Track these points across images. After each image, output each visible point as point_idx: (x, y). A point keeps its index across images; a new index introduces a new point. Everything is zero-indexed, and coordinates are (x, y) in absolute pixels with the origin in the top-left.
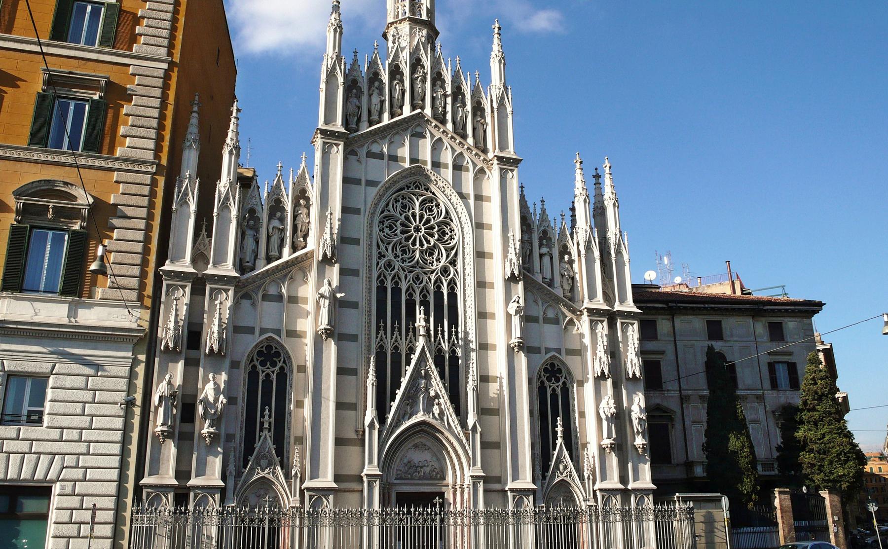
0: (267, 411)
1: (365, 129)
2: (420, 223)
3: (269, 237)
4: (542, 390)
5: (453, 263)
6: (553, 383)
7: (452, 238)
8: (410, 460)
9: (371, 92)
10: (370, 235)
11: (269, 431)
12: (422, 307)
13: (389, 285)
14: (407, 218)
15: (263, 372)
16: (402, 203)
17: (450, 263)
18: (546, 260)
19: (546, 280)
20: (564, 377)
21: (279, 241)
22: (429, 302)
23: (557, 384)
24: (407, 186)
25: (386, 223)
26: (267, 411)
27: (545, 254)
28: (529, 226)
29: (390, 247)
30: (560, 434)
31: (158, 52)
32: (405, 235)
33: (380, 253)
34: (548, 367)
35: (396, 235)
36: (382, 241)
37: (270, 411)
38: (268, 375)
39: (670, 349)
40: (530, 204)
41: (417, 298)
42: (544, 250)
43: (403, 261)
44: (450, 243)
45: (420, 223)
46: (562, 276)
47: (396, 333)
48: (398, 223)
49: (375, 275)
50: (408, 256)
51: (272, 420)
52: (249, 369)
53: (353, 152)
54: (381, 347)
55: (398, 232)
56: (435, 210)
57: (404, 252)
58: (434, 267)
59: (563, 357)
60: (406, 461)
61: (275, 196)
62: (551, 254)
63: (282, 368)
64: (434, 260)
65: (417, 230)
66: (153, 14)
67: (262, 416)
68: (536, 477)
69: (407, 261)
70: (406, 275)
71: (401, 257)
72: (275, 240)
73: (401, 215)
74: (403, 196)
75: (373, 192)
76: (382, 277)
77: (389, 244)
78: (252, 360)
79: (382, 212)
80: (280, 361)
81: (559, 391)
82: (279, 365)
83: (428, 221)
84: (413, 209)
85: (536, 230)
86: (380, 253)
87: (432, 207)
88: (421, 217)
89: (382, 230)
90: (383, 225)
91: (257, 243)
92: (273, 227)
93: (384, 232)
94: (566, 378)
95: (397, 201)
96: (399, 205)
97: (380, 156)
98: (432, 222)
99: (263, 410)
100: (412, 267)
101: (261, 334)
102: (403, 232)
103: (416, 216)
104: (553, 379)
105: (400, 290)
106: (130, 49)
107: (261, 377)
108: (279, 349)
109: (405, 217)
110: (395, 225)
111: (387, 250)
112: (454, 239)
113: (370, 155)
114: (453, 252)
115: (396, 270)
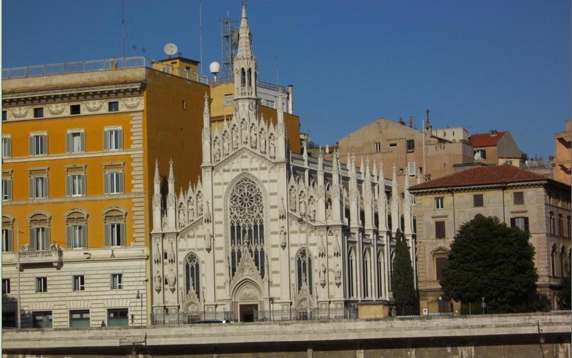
5: (262, 212)
13: (235, 225)
41: (247, 229)
43: (241, 214)
49: (229, 221)
57: (241, 210)
72: (191, 213)
75: (226, 187)
97: (229, 171)
113: (225, 171)
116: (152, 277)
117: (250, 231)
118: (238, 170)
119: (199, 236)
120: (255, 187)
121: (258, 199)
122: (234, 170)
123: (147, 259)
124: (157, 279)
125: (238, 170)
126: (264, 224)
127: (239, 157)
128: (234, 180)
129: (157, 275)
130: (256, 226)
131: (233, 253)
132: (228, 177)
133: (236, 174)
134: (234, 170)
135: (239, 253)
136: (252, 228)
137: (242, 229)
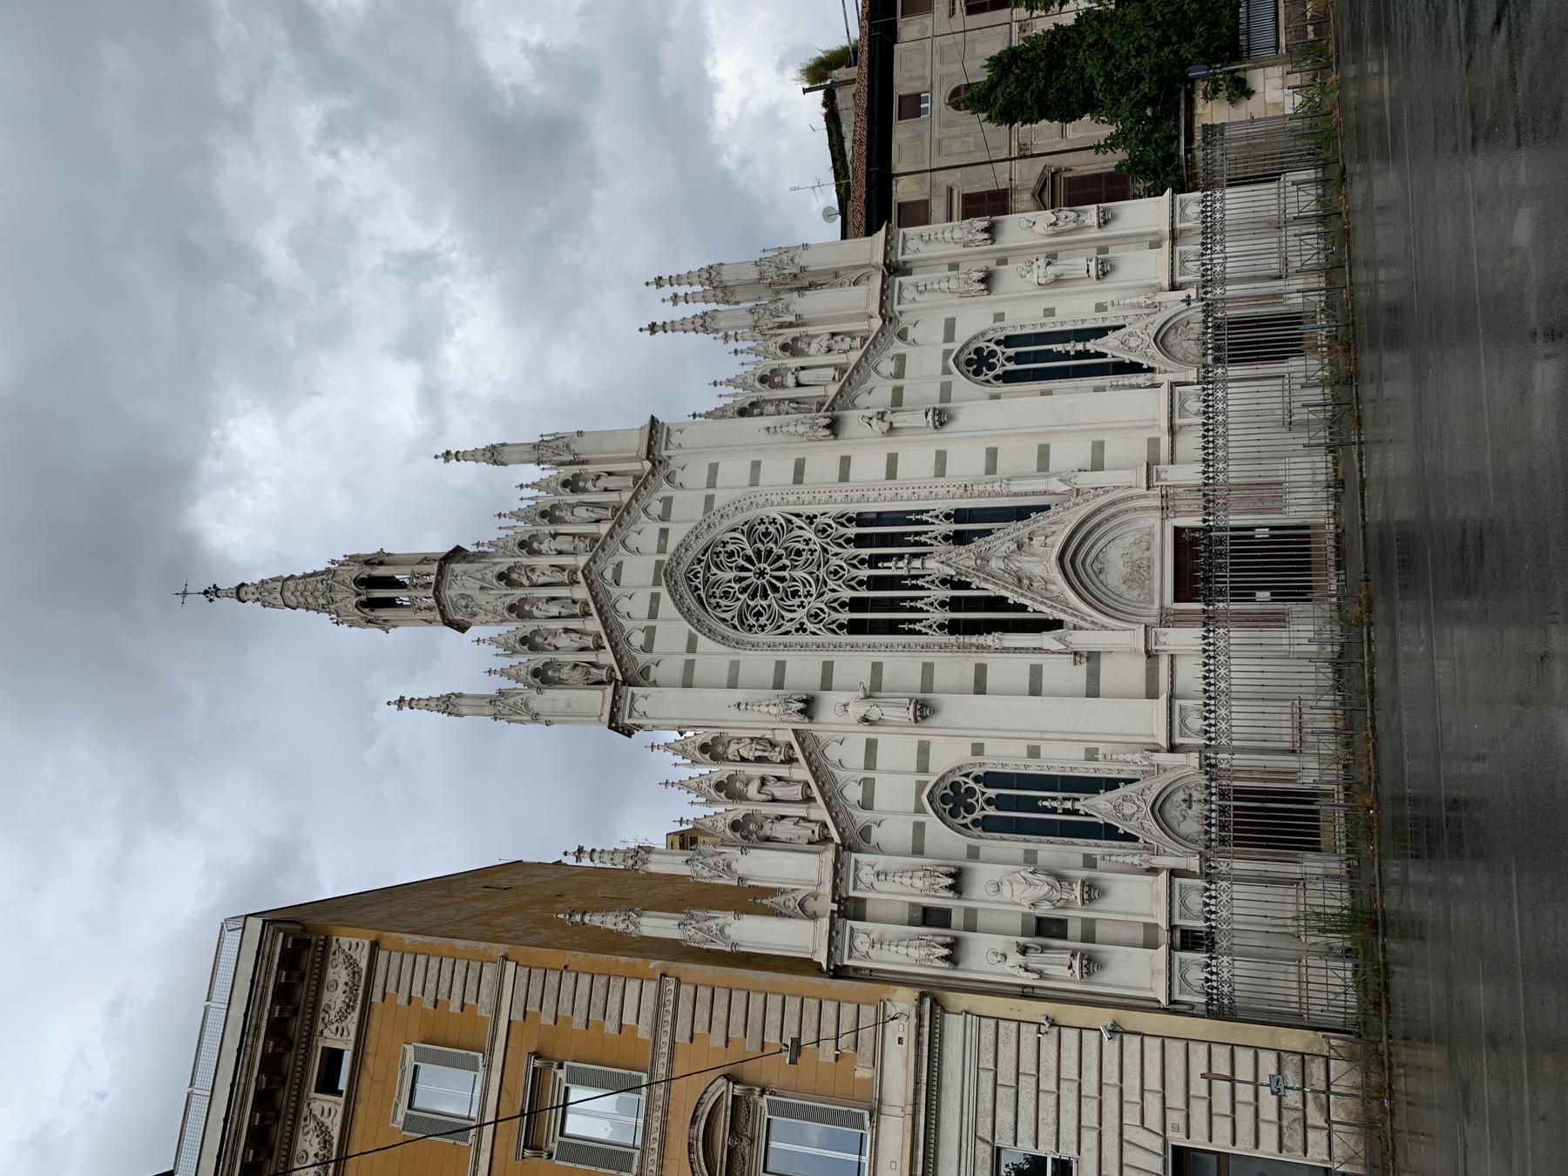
0: (1045, 803)
1: (607, 658)
2: (750, 570)
3: (774, 800)
4: (1008, 378)
5: (811, 519)
6: (998, 360)
7: (774, 522)
8: (1121, 581)
9: (550, 648)
10: (771, 646)
11: (1078, 800)
12: (880, 565)
13: (845, 616)
14: (744, 590)
15: (983, 809)
16: (721, 598)
17: (812, 523)
18: (804, 377)
19: (837, 377)
20: (988, 344)
21: (780, 783)
22: (871, 556)
23: (1000, 354)
24: (695, 591)
25: (752, 621)
26: (1045, 803)
27: (796, 378)
28: (753, 404)
29: (788, 615)
30: (1080, 347)
31: (489, 977)
32: (769, 592)
33: (797, 630)
34: (971, 369)
35: (769, 606)
36: (779, 627)
37: (1045, 799)
38: (989, 801)
39: (943, 178)
40: (720, 403)
41: (865, 573)
42: (790, 380)
43: (809, 594)
44: (781, 524)
45: (750, 570)
46: (829, 350)
47: (919, 604)
48: (752, 603)
49: (828, 638)
50: (801, 588)
51: (1060, 795)
52: (978, 831)
53: (645, 673)
54: (941, 627)
55: (764, 603)
56: (730, 547)
57: (795, 594)
58: (818, 548)
59: (956, 346)
60: (1124, 588)
61: (712, 791)
62: (796, 369)
63: (977, 779)
64: (806, 548)
65: (762, 573)
66: (431, 986)
67: (1054, 811)
68: (1149, 383)
69: (809, 588)
70: (830, 590)
71: (803, 599)
72: (778, 790)
73: (738, 599)
74: (710, 597)
75: (703, 642)
76: (833, 626)
77: (783, 617)
78: (965, 826)
79: (735, 627)
80: (966, 783)
81: (1011, 352)
82: (971, 784)
83: (748, 559)
84: (730, 581)
85: (758, 394)
86: (797, 630)
87: (726, 552)
88: (742, 569)
89: (763, 628)
90: (754, 626)
91: (783, 817)
92: (759, 792)
93: (766, 625)
94: (990, 341)
95: (718, 605)
96: (723, 602)
97: (650, 632)
98: (750, 552)
99: (1045, 810)
100: (817, 580)
101: (924, 812)
102: (765, 596)
103: (740, 577)
104: (991, 361)
105: (852, 599)
106: (485, 1019)
107: (991, 811)
109: (741, 593)
110: (754, 609)
111: (792, 620)
112: (774, 519)
114: (794, 519)
115: (823, 606)
116: (1026, 993)
117: (873, 562)
118: (655, 598)
119: (870, 763)
120: (724, 544)
121: (766, 534)
122: (653, 614)
123: (935, 1002)
124: (1034, 959)
125: (655, 598)
126: (853, 509)
127: (615, 591)
128: (687, 614)
129: (1015, 958)
130: (860, 541)
131: (953, 628)
132: (673, 629)
133: (667, 604)
134: (653, 614)
135: (954, 604)
136: (865, 552)
137: (864, 593)
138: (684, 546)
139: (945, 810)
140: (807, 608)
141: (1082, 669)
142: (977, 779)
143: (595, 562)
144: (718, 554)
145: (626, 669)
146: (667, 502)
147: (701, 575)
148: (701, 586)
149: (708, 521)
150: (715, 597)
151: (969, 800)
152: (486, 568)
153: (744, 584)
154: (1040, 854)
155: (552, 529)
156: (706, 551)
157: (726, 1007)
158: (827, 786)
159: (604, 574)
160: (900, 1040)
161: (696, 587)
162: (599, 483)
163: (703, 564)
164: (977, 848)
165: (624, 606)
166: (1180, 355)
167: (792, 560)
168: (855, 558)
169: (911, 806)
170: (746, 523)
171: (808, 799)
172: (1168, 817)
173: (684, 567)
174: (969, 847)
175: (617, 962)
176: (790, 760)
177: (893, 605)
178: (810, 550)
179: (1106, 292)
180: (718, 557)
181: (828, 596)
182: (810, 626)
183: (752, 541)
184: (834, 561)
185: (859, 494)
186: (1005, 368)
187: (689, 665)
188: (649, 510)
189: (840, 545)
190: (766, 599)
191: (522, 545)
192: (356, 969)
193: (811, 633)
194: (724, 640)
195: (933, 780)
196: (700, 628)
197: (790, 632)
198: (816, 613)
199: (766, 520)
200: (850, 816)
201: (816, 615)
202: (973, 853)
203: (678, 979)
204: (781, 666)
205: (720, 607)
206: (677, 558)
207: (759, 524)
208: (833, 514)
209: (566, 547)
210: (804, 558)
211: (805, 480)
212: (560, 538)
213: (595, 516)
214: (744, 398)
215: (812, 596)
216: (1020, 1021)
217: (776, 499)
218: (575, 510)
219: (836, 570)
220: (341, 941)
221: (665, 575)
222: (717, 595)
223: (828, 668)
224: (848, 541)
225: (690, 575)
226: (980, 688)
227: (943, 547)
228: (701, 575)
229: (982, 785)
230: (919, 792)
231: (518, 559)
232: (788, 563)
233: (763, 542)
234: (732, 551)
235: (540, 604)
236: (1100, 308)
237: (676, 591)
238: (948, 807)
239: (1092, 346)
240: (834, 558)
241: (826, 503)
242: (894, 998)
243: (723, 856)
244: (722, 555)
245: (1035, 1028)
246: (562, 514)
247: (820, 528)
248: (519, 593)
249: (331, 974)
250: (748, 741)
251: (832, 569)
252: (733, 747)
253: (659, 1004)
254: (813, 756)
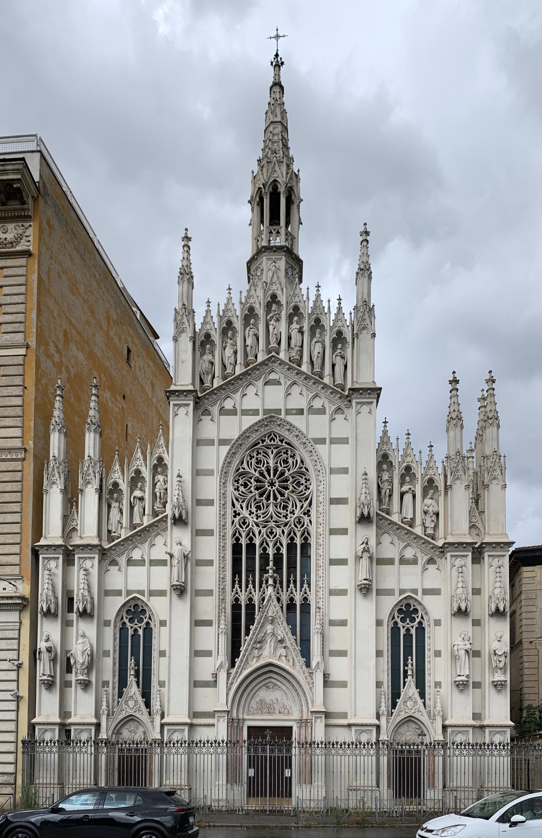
5: (307, 513)
13: (244, 541)
24: (262, 440)
29: (244, 505)
31: (16, 338)
33: (235, 512)
35: (251, 492)
36: (237, 500)
41: (271, 551)
44: (305, 493)
49: (230, 531)
50: (262, 511)
53: (207, 412)
54: (237, 600)
56: (290, 460)
57: (258, 508)
58: (288, 520)
65: (272, 484)
66: (9, 300)
70: (260, 530)
74: (258, 452)
75: (225, 450)
76: (237, 534)
77: (244, 501)
83: (282, 474)
84: (268, 463)
86: (235, 512)
87: (287, 458)
90: (238, 483)
93: (238, 491)
95: (252, 457)
96: (254, 461)
97: (233, 412)
101: (127, 596)
102: (257, 489)
108: (145, 608)
111: (242, 508)
112: (309, 489)
119: (155, 563)
120: (293, 456)
121: (299, 484)
122: (245, 412)
123: (25, 606)
125: (255, 412)
126: (312, 541)
127: (260, 383)
128: (244, 436)
130: (291, 547)
131: (236, 606)
134: (245, 412)
135: (250, 606)
136: (284, 551)
137: (258, 551)
138: (291, 428)
139: (130, 607)
140: (248, 516)
141: (210, 678)
142: (148, 624)
143: (280, 364)
144: (286, 453)
145: (208, 399)
146: (322, 411)
147: (272, 442)
148: (265, 443)
149: (307, 442)
150: (257, 455)
151: (136, 620)
152: (280, 284)
153: (266, 473)
154: (108, 658)
155: (306, 329)
156: (289, 444)
157: (12, 490)
158: (139, 538)
159: (273, 374)
160: (4, 589)
161: (265, 441)
162: (338, 358)
163: (280, 443)
164: (109, 626)
165: (251, 391)
166: (401, 730)
167: (281, 504)
168: (281, 544)
169: (130, 588)
170: (307, 470)
171: (133, 526)
172: (131, 723)
173: (277, 430)
174: (110, 621)
175: (31, 421)
176: (155, 514)
177: (251, 570)
178: (287, 515)
179: (447, 688)
180: (284, 453)
181: (256, 530)
182: (237, 520)
183: (294, 475)
184: (278, 531)
185: (321, 543)
186: (402, 628)
187: (211, 442)
188: (317, 398)
189: (289, 534)
190: (255, 489)
191: (296, 308)
192: (14, 244)
193: (233, 521)
194: (228, 463)
195: (145, 599)
196: (236, 445)
197: (234, 507)
198: (246, 523)
199: (308, 483)
200: (123, 553)
201: (244, 523)
202: (107, 623)
203: (24, 459)
204: (210, 503)
205: (251, 459)
206: (284, 424)
207: (306, 479)
208: (310, 528)
209: (293, 342)
210: (282, 511)
211: (333, 506)
212: (299, 335)
213: (314, 359)
214: (396, 458)
215: (257, 519)
216: (19, 650)
217: (321, 488)
218: (319, 344)
219: (273, 532)
220: (31, 229)
221: (270, 417)
222: (259, 456)
223: (209, 533)
224: (292, 539)
225: (273, 435)
226: (197, 623)
227: (285, 598)
228: (272, 442)
229: (145, 626)
230: (139, 592)
231: (284, 306)
232: (278, 501)
233: (293, 483)
234: (288, 462)
235: (253, 330)
236: (438, 684)
237: (261, 426)
238: (132, 608)
239: (411, 681)
240: (281, 531)
241: (317, 522)
242: (25, 584)
243: (93, 478)
244: (285, 455)
245: (16, 658)
246: (317, 335)
247: (302, 520)
248: (260, 311)
249: (10, 226)
250: (165, 487)
251: (274, 530)
252: (160, 478)
253: (10, 450)
254: (156, 528)
